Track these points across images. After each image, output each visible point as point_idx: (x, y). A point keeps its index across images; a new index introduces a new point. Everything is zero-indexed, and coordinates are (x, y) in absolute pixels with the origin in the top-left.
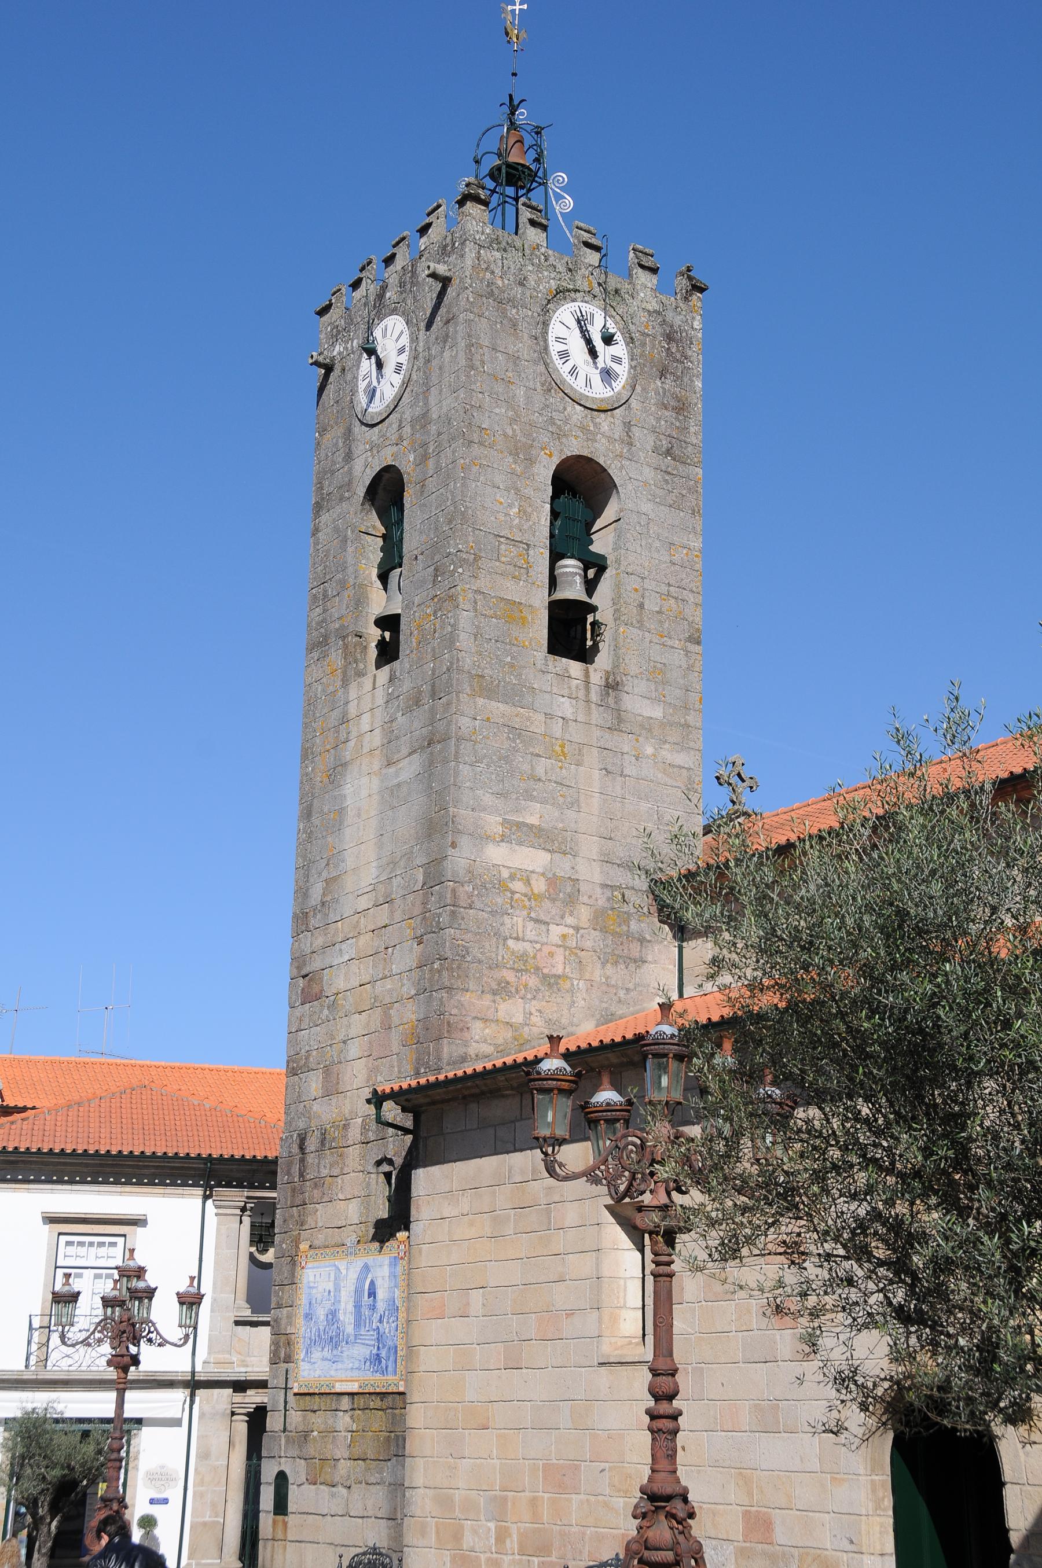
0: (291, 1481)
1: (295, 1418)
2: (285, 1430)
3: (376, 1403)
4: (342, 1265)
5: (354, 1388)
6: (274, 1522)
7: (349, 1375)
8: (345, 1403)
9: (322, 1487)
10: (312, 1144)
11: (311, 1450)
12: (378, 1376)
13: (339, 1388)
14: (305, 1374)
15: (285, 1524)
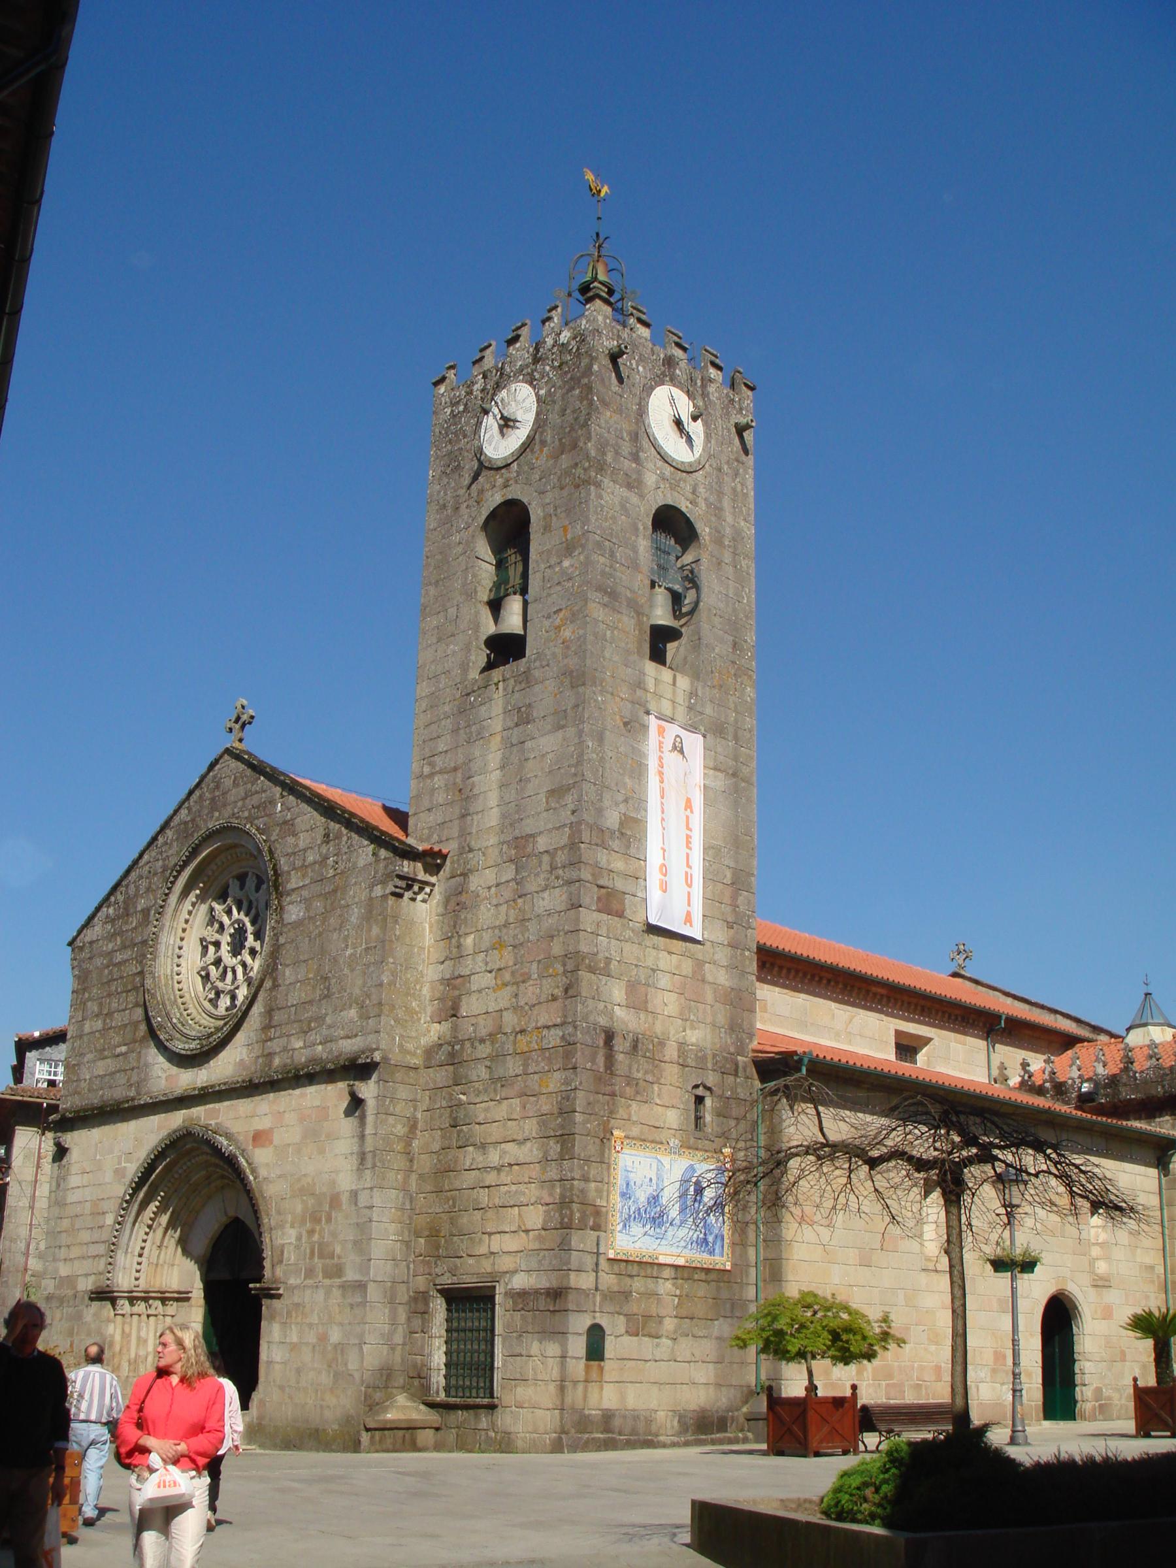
0: (607, 1332)
1: (608, 1280)
2: (597, 1289)
3: (703, 1276)
4: (666, 1160)
5: (681, 1262)
6: (587, 1367)
7: (675, 1251)
8: (667, 1273)
9: (646, 1339)
10: (620, 1045)
11: (633, 1308)
12: (705, 1256)
13: (662, 1260)
14: (624, 1244)
15: (601, 1369)
